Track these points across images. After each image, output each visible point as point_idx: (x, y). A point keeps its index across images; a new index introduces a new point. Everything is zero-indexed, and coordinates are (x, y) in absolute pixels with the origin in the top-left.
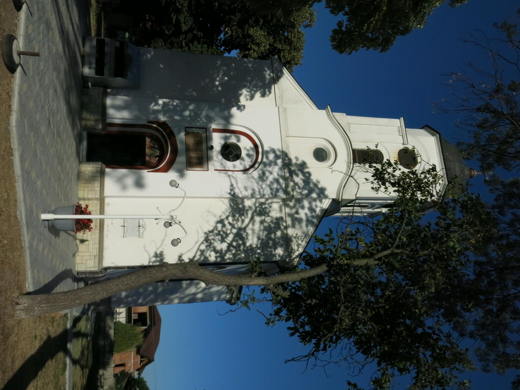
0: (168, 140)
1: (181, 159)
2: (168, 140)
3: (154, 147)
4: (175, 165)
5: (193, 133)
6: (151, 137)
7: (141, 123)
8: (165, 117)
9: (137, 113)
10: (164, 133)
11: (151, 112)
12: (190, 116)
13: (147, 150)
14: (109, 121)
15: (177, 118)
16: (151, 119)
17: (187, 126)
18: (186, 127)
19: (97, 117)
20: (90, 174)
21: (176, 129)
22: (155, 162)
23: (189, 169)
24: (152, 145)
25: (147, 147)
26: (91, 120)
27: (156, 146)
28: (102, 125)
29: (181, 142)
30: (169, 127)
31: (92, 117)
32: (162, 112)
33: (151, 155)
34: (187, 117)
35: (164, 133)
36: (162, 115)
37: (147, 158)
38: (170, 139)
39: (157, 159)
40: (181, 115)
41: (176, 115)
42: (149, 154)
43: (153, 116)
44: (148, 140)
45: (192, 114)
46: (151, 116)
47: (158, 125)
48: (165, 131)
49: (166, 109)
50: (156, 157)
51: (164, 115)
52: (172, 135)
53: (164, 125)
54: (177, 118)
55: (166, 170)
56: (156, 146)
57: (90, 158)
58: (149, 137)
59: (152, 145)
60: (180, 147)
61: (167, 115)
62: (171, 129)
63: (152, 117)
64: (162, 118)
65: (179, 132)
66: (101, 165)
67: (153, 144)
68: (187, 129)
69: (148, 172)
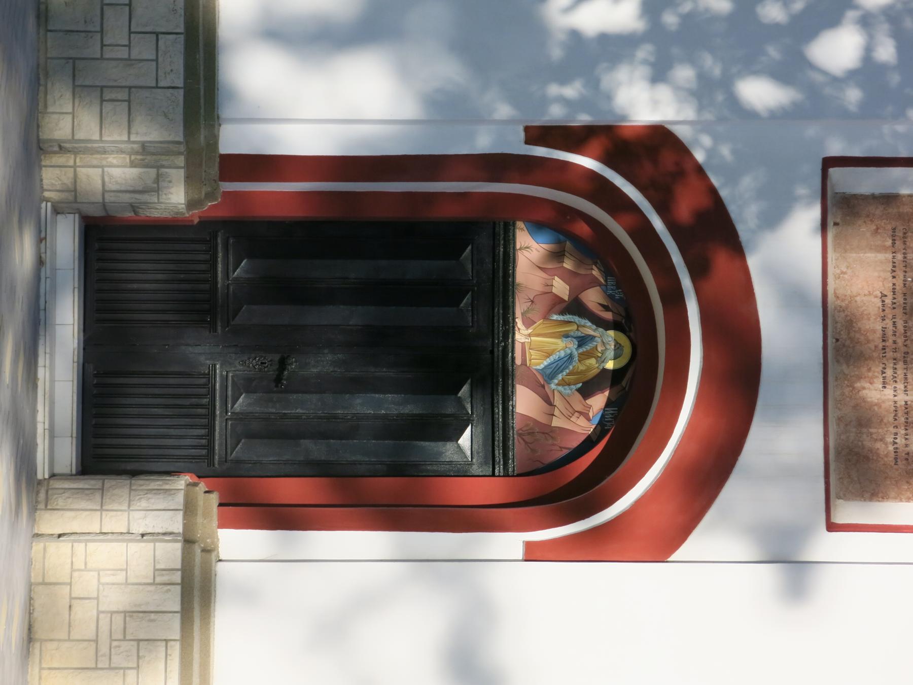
0: (686, 282)
1: (786, 441)
2: (686, 282)
3: (575, 307)
4: (734, 493)
5: (889, 199)
6: (556, 223)
7: (483, 142)
8: (664, 92)
9: (447, 71)
10: (658, 224)
11: (557, 53)
12: (867, 71)
13: (522, 335)
14: (235, 139)
15: (759, 92)
16: (556, 114)
17: (836, 148)
18: (829, 163)
19: (149, 132)
20: (116, 599)
21: (747, 182)
22: (584, 427)
23: (846, 513)
24: (561, 288)
25: (520, 308)
26: (109, 156)
27: (593, 298)
28: (189, 179)
29: (793, 296)
30: (700, 170)
31: (116, 135)
32: (644, 52)
33: (550, 373)
34: (839, 81)
35: (658, 224)
36: (643, 71)
37: (525, 402)
38: (699, 271)
39: (598, 402)
40: (792, 68)
41: (751, 68)
42: (538, 363)
43: (571, 91)
44: (530, 249)
45: (886, 52)
46: (554, 90)
47: (608, 160)
48: (663, 210)
49: (670, 19)
50: (587, 390)
51: (659, 74)
52: (713, 234)
53: (652, 154)
54: (759, 92)
55: (659, 537)
56: (593, 298)
57: (108, 452)
58: (537, 226)
59: (561, 288)
60: (785, 336)
61: (684, 74)
62: (713, 192)
63: (563, 102)
64: (642, 103)
65: (774, 218)
66: (189, 509)
67: (568, 277)
68: (835, 173)
69: (533, 553)
